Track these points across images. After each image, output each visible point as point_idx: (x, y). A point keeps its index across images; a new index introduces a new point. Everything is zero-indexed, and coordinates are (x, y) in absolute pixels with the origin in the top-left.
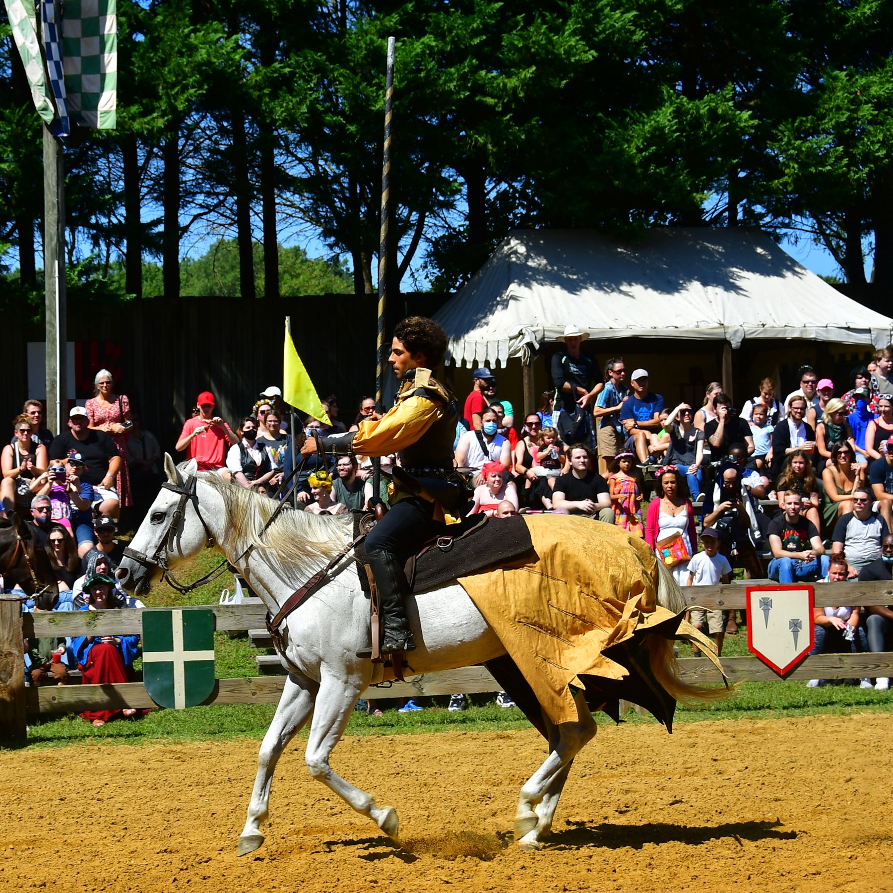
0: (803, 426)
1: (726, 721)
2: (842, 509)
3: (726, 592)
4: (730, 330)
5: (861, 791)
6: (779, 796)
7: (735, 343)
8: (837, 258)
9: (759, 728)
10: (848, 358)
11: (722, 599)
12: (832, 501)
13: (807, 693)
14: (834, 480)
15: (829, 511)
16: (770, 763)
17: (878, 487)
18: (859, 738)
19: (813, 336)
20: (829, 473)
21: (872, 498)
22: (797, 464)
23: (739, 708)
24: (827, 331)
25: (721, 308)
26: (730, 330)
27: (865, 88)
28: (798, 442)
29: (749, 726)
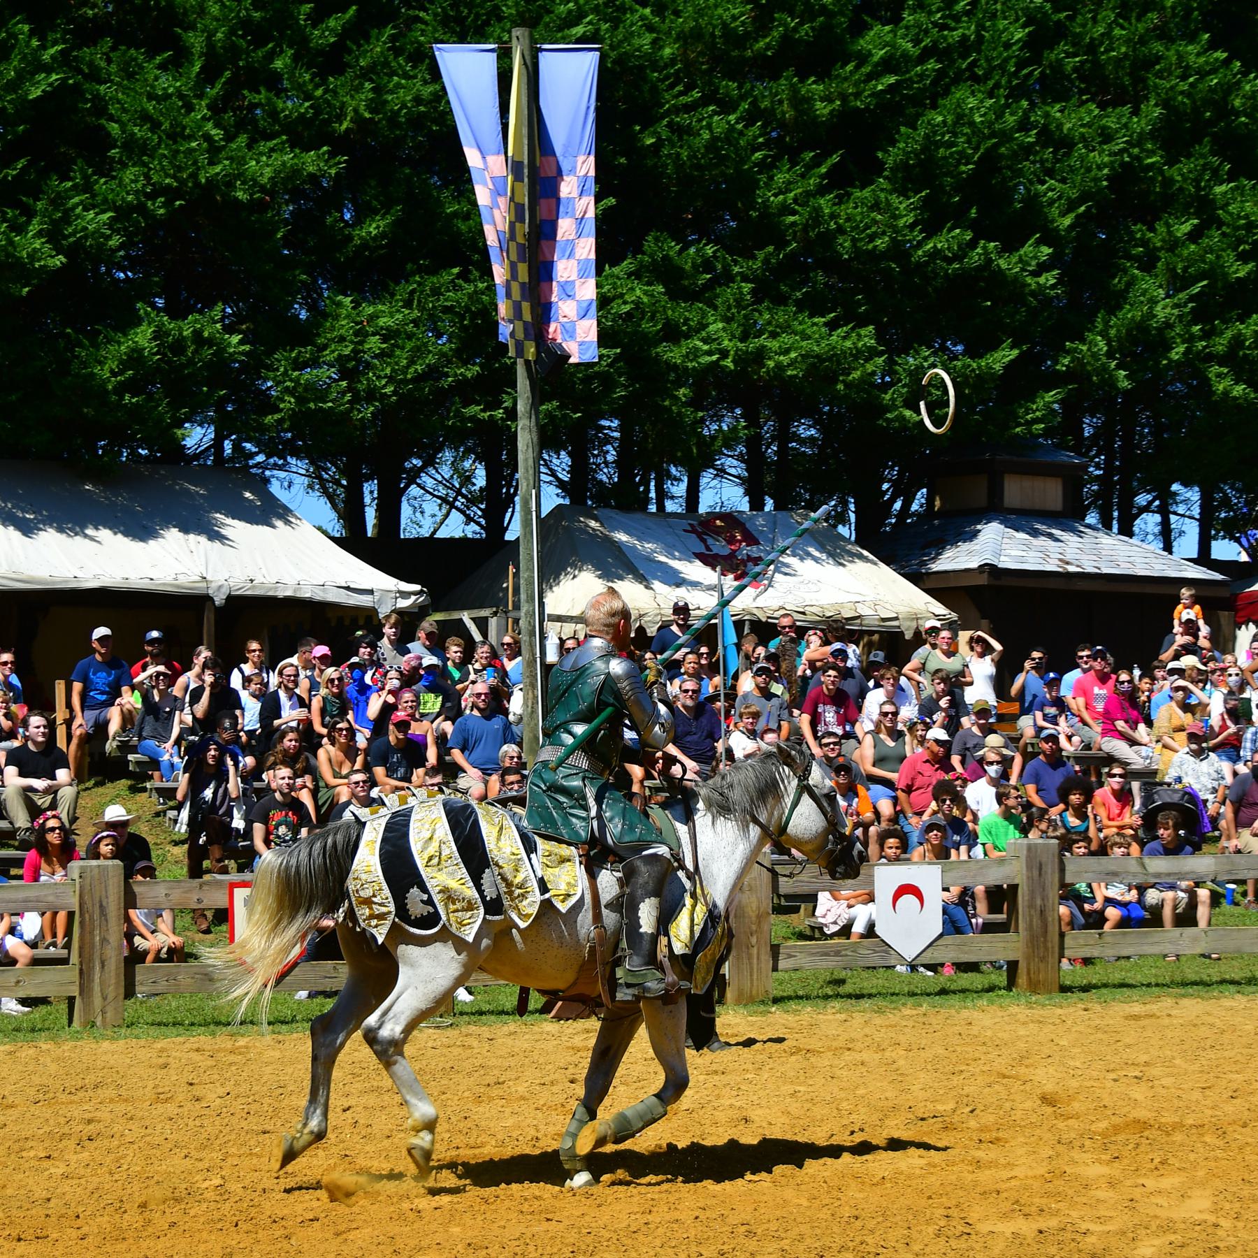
0: (295, 698)
1: (202, 1037)
2: (338, 794)
3: (205, 888)
4: (214, 585)
5: (362, 1121)
6: (267, 1127)
7: (219, 600)
8: (334, 506)
9: (241, 1047)
10: (347, 622)
11: (201, 895)
12: (327, 786)
13: (295, 1006)
14: (330, 760)
15: (323, 795)
16: (255, 1088)
17: (379, 771)
18: (355, 1060)
19: (308, 595)
20: (327, 753)
21: (372, 782)
22: (289, 742)
23: (218, 1023)
24: (324, 591)
25: (203, 560)
26: (214, 585)
27: (373, 318)
28: (290, 715)
29: (229, 1045)
